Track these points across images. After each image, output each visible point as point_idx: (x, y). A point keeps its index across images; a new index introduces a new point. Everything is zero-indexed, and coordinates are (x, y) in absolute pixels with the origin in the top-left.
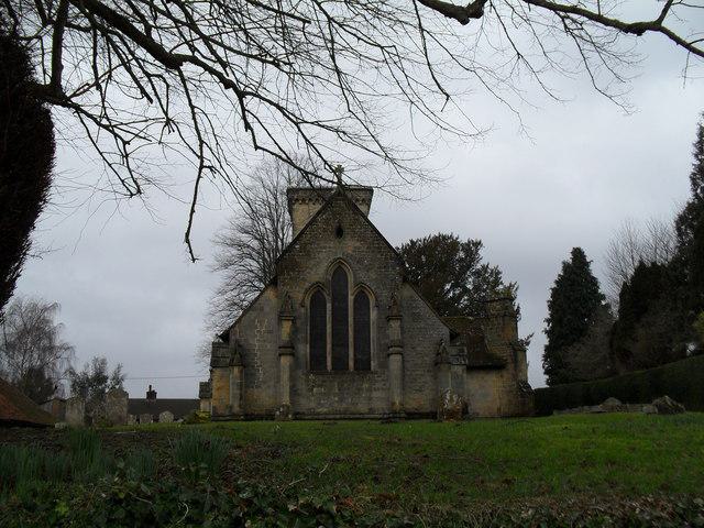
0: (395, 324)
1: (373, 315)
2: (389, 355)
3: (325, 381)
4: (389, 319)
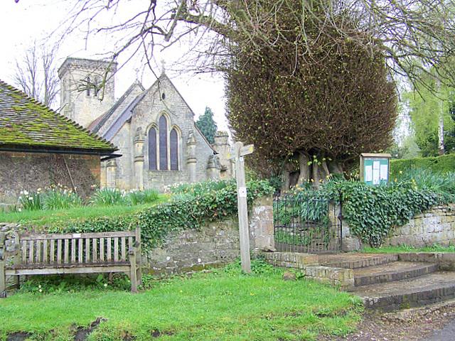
0: (193, 147)
1: (180, 141)
2: (188, 163)
4: (188, 144)
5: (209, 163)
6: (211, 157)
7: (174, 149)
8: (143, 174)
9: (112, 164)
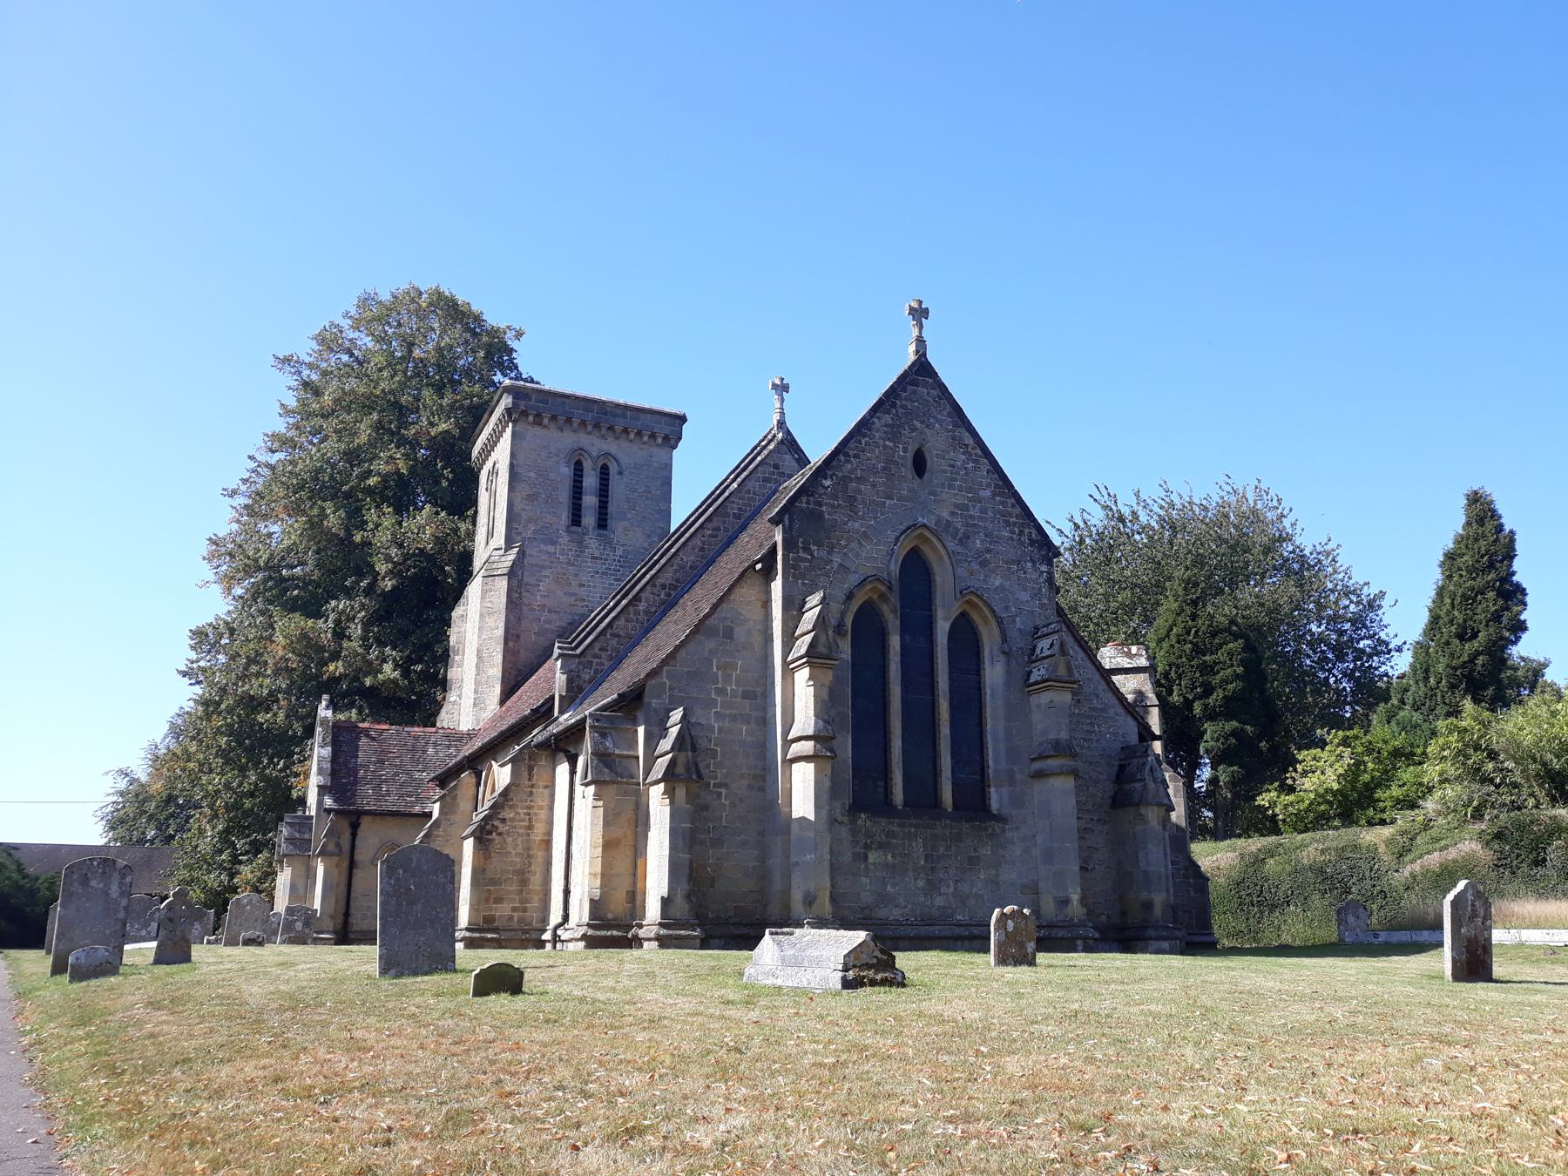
1: (994, 674)
2: (1040, 775)
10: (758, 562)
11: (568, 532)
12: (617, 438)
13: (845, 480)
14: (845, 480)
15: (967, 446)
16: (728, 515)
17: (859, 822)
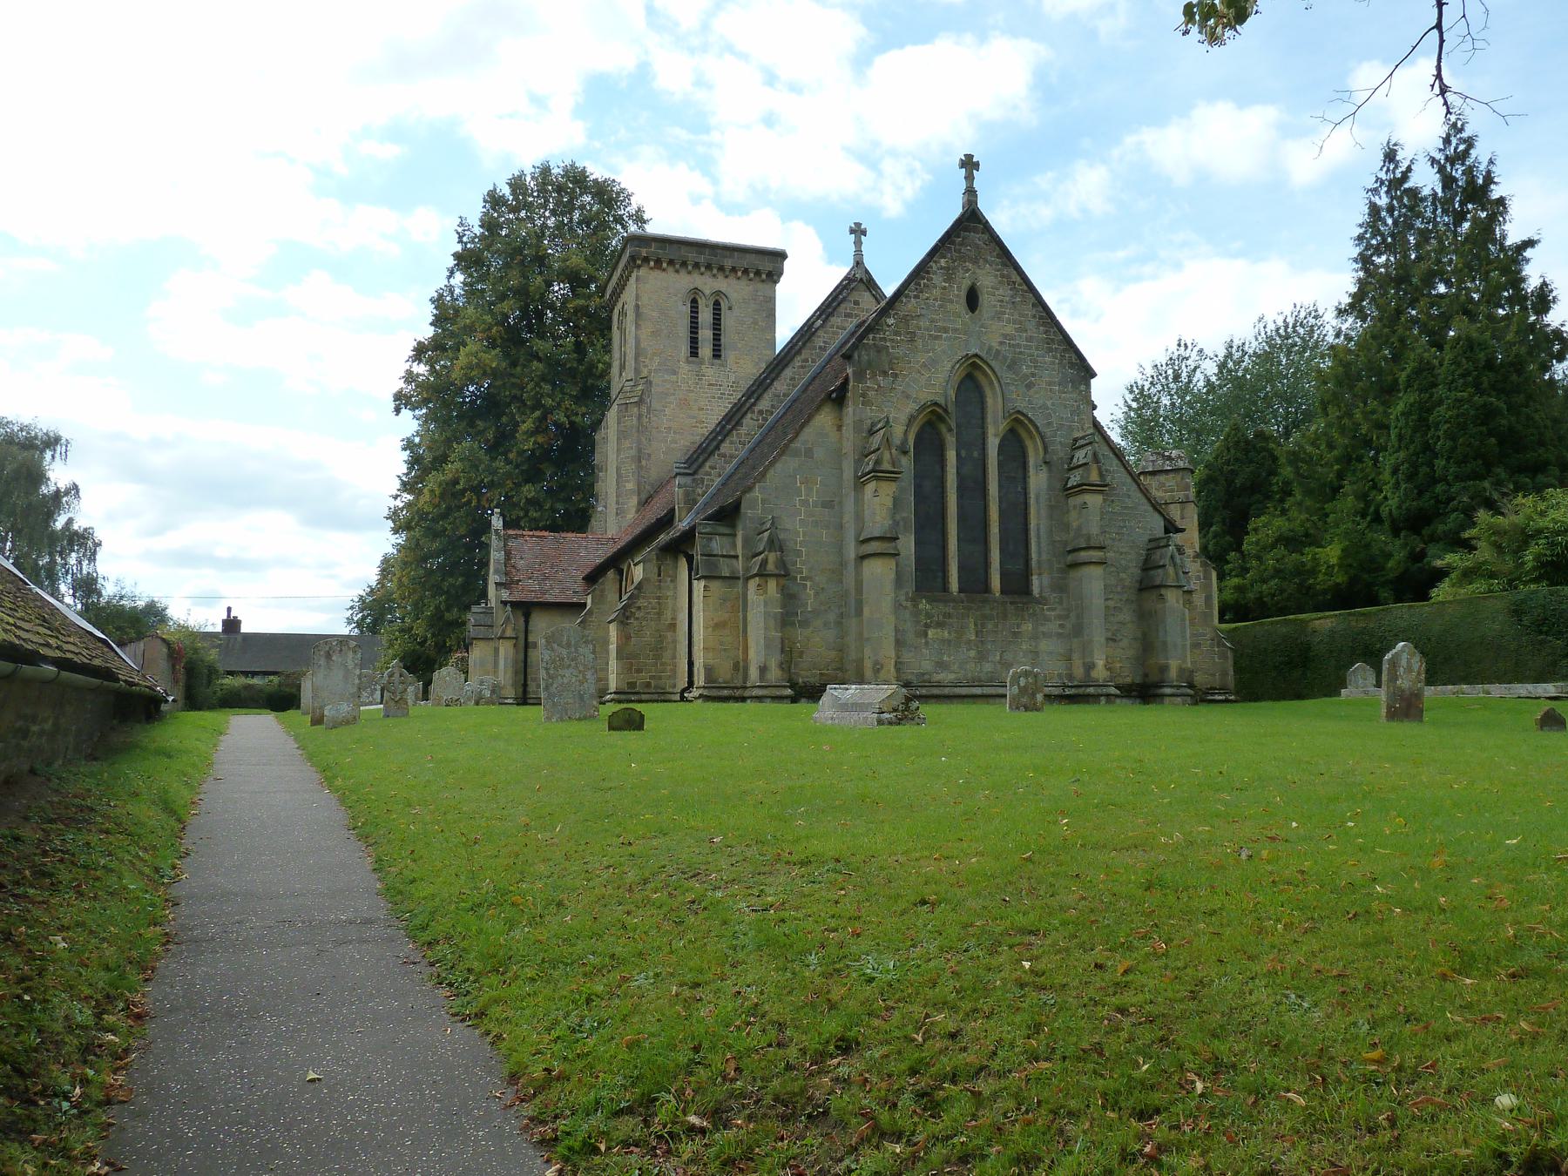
0: (1094, 500)
1: (1038, 480)
2: (1075, 565)
3: (950, 616)
4: (1069, 491)
5: (1148, 566)
6: (1155, 545)
7: (1016, 512)
8: (898, 606)
9: (771, 567)
10: (833, 391)
11: (688, 362)
12: (726, 277)
13: (905, 320)
14: (905, 320)
15: (1014, 283)
16: (815, 348)
17: (920, 606)
